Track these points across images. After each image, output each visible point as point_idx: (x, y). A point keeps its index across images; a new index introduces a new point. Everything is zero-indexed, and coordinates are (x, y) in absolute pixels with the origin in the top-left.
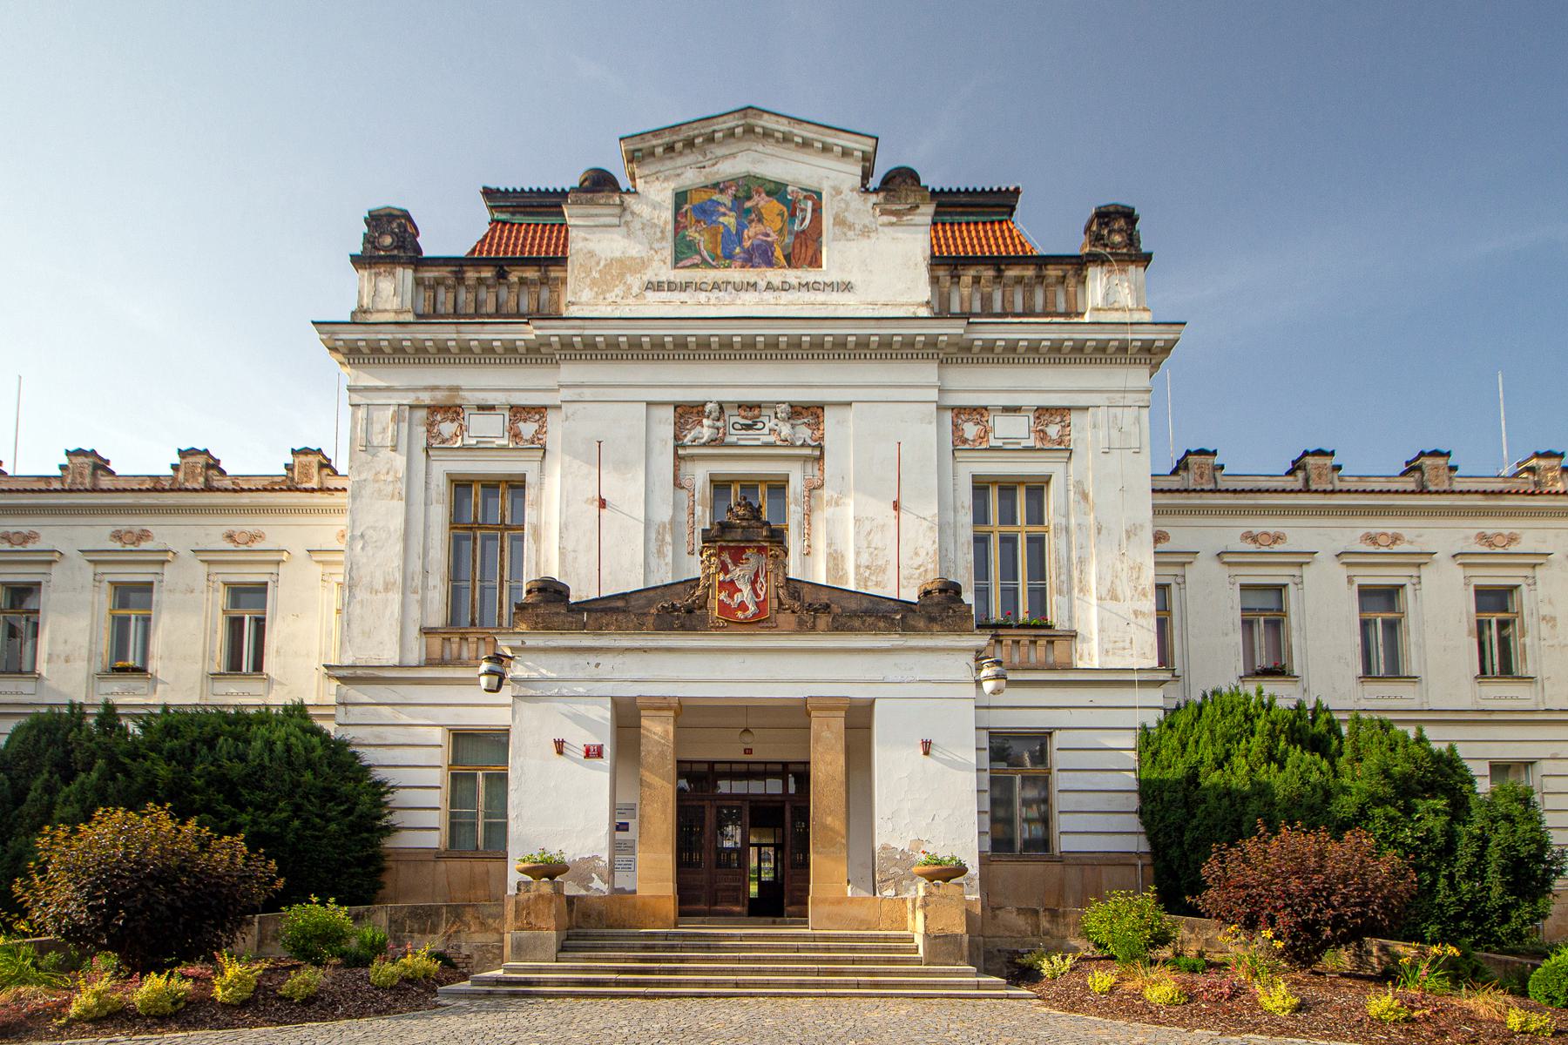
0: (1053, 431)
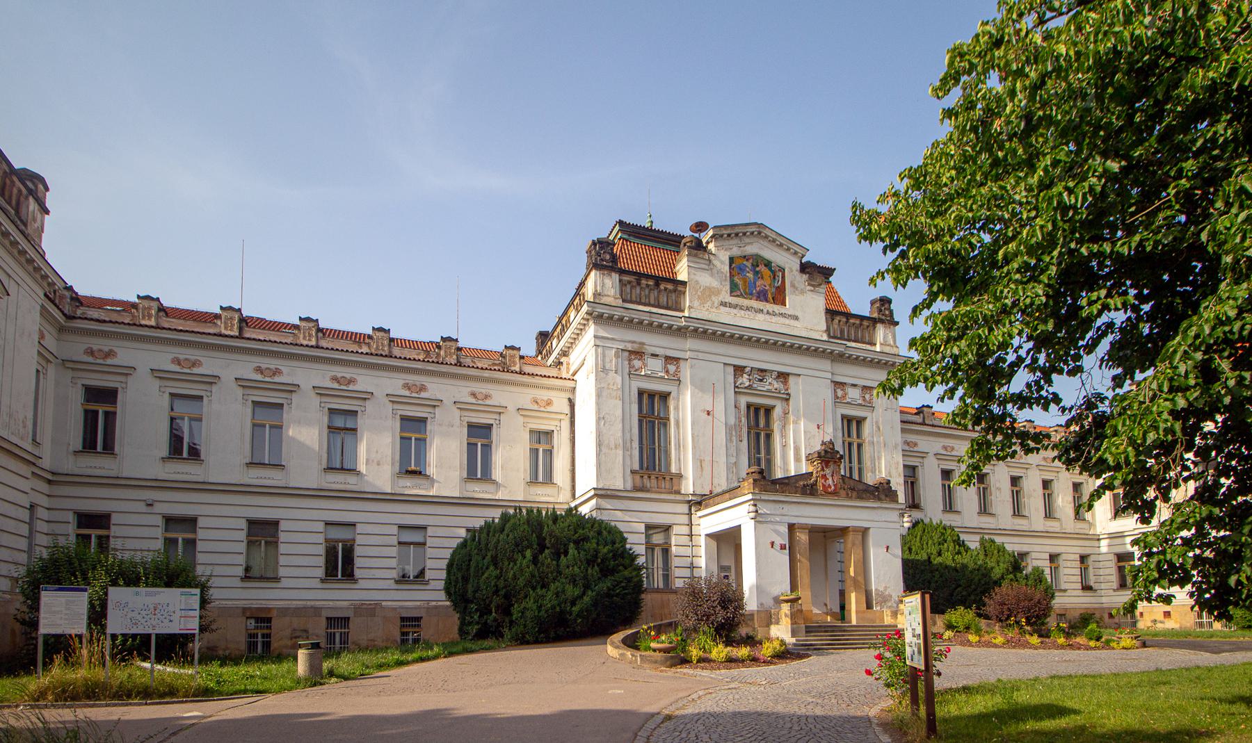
0: (867, 396)
